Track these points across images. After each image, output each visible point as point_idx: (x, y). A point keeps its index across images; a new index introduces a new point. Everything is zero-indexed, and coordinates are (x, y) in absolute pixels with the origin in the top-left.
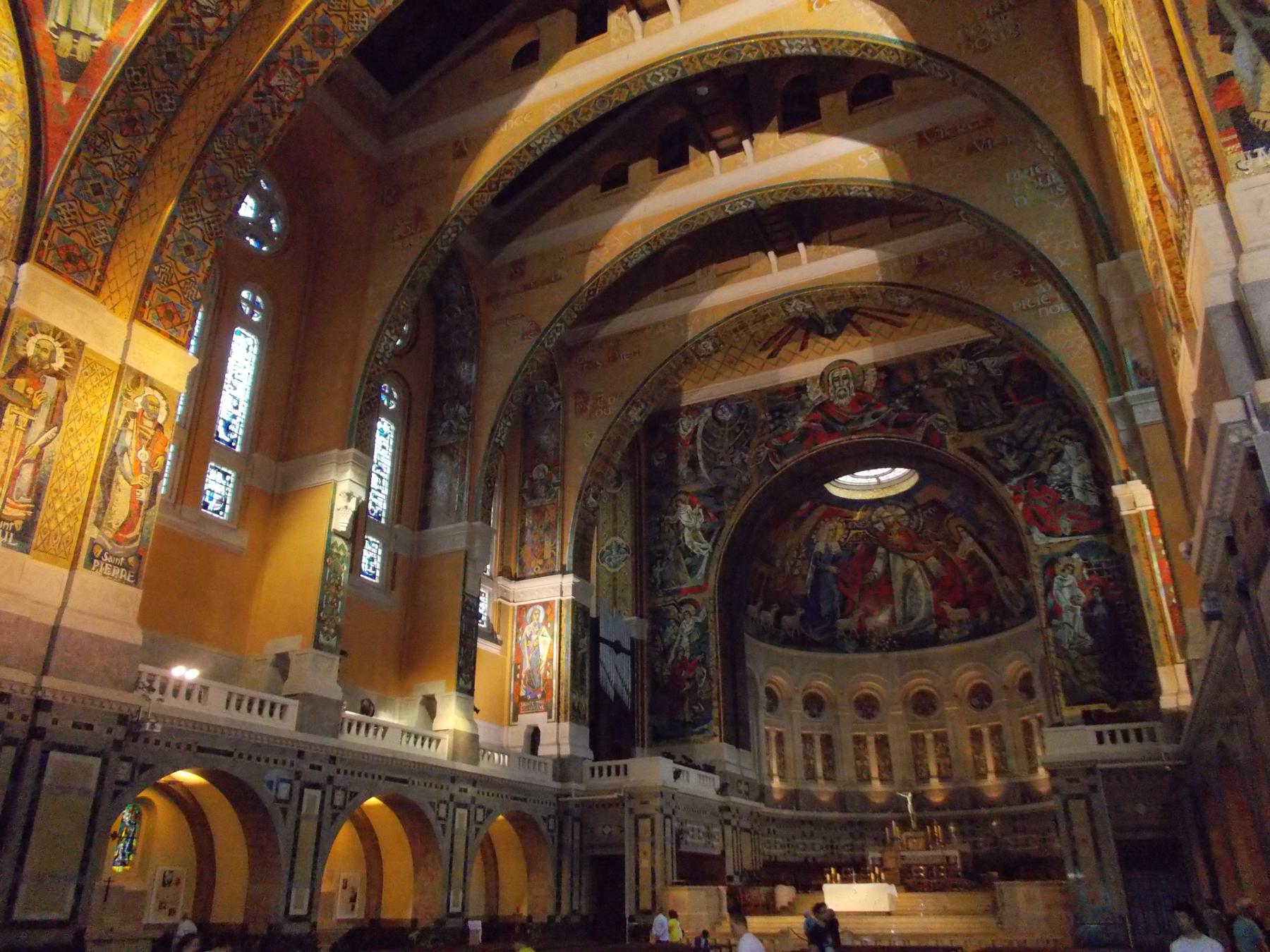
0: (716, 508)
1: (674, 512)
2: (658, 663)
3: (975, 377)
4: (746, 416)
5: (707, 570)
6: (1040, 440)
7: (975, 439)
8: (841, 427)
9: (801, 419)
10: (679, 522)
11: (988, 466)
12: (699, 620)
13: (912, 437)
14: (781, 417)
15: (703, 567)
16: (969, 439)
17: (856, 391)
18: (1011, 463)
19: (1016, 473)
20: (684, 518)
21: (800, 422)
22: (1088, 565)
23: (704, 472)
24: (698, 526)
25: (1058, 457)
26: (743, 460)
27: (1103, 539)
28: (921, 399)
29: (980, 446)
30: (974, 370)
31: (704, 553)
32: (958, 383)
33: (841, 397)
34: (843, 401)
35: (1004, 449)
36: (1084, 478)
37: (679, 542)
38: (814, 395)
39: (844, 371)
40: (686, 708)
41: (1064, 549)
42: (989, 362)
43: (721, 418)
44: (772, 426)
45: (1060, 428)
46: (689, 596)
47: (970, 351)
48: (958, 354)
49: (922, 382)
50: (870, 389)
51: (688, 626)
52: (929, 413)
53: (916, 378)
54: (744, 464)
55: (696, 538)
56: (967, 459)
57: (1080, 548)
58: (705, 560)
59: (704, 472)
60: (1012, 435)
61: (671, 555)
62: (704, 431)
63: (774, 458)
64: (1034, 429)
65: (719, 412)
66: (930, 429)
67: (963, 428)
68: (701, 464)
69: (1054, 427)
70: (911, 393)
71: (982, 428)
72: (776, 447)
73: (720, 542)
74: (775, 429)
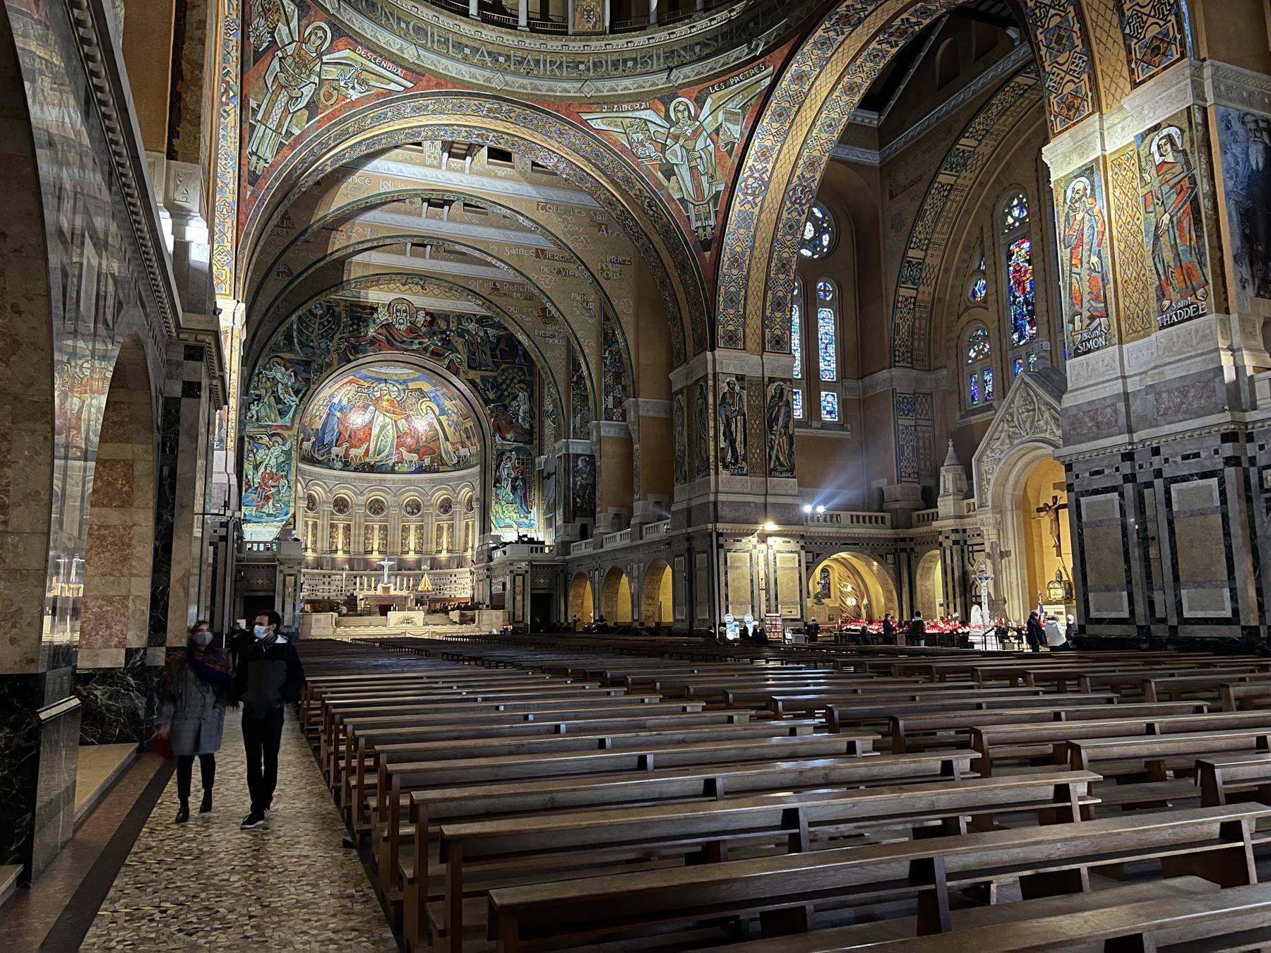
0: (304, 375)
1: (271, 370)
3: (481, 337)
4: (333, 315)
5: (294, 416)
6: (508, 386)
14: (359, 325)
15: (291, 414)
16: (472, 375)
18: (492, 395)
20: (279, 376)
22: (518, 459)
26: (328, 346)
27: (528, 446)
28: (449, 341)
30: (482, 334)
31: (293, 404)
34: (402, 327)
38: (382, 316)
41: (508, 448)
42: (490, 331)
43: (314, 311)
45: (519, 382)
47: (481, 321)
57: (517, 450)
58: (293, 409)
60: (495, 378)
61: (266, 400)
66: (452, 361)
67: (469, 367)
68: (295, 341)
69: (516, 381)
73: (305, 399)
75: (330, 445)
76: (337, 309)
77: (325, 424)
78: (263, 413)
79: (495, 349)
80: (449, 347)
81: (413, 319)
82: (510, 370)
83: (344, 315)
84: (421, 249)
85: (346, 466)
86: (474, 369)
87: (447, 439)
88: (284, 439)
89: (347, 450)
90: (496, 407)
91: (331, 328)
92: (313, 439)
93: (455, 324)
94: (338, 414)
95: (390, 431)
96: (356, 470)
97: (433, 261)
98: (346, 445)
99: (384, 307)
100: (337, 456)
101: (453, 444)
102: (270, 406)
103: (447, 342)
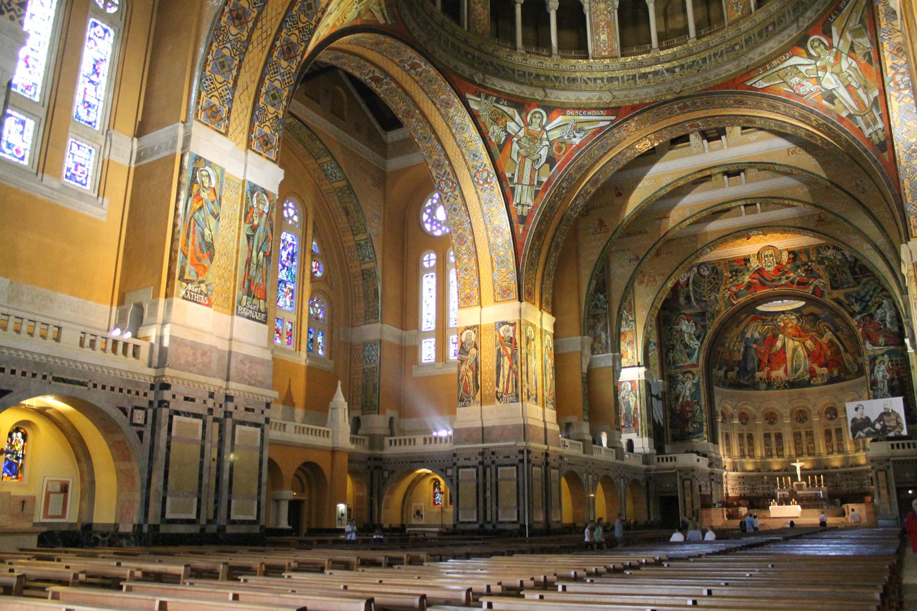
1: (678, 324)
2: (673, 403)
3: (840, 260)
4: (717, 273)
6: (871, 297)
7: (839, 294)
8: (769, 283)
9: (747, 277)
10: (681, 330)
11: (845, 308)
12: (695, 382)
13: (807, 291)
14: (736, 276)
15: (696, 355)
16: (836, 294)
17: (777, 263)
18: (857, 308)
19: (860, 313)
20: (684, 328)
21: (747, 279)
23: (694, 303)
24: (692, 332)
25: (880, 306)
26: (716, 298)
28: (812, 270)
29: (842, 298)
30: (840, 257)
31: (696, 347)
32: (831, 263)
33: (769, 267)
35: (853, 300)
36: (892, 317)
37: (682, 341)
38: (754, 264)
39: (770, 252)
40: (689, 425)
43: (703, 274)
44: (731, 280)
46: (691, 369)
48: (831, 247)
49: (812, 261)
50: (784, 263)
51: (689, 385)
52: (816, 278)
53: (809, 257)
54: (717, 301)
55: (691, 339)
56: (835, 304)
59: (694, 303)
61: (678, 347)
62: (694, 280)
63: (733, 298)
64: (868, 291)
65: (702, 270)
67: (833, 288)
68: (693, 299)
70: (806, 267)
71: (843, 288)
72: (733, 292)
73: (705, 342)
74: (733, 281)
75: (753, 371)
76: (719, 268)
77: (745, 355)
78: (677, 358)
79: (854, 267)
80: (812, 275)
81: (778, 261)
82: (871, 282)
83: (724, 270)
84: (753, 207)
85: (770, 385)
86: (837, 288)
87: (846, 351)
88: (693, 374)
89: (769, 373)
90: (863, 318)
91: (716, 283)
92: (737, 369)
93: (815, 254)
94: (754, 346)
95: (801, 352)
96: (778, 388)
97: (764, 214)
98: (767, 369)
99: (754, 257)
100: (761, 379)
101: (852, 355)
102: (681, 352)
103: (810, 272)
